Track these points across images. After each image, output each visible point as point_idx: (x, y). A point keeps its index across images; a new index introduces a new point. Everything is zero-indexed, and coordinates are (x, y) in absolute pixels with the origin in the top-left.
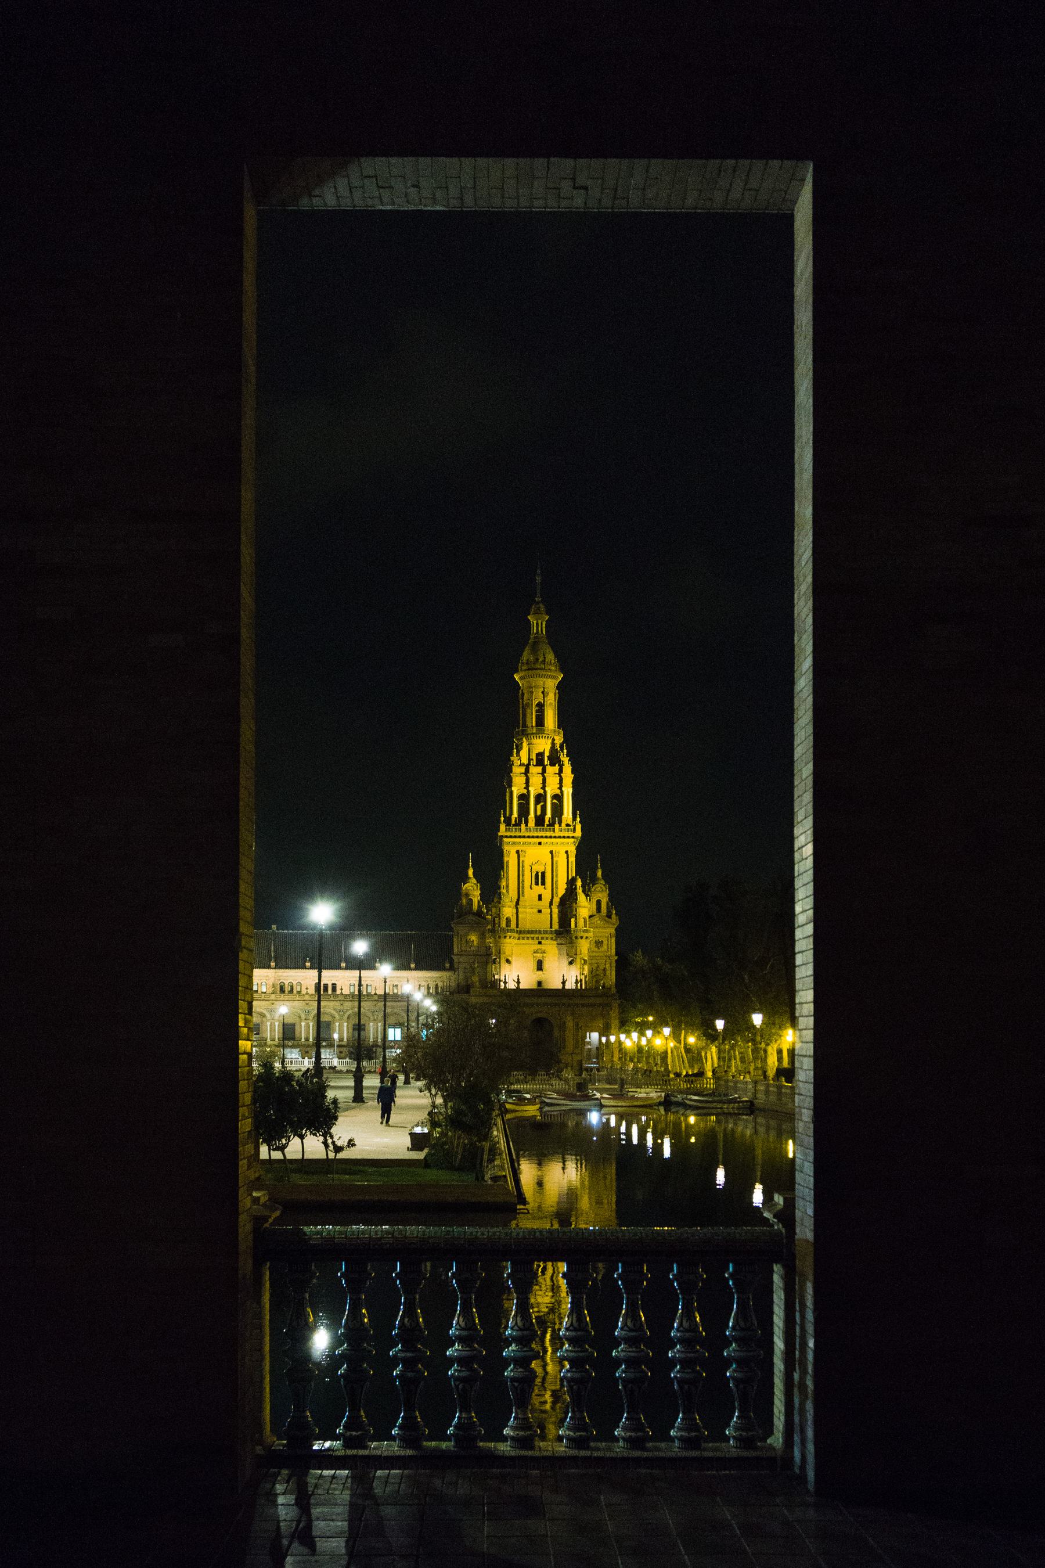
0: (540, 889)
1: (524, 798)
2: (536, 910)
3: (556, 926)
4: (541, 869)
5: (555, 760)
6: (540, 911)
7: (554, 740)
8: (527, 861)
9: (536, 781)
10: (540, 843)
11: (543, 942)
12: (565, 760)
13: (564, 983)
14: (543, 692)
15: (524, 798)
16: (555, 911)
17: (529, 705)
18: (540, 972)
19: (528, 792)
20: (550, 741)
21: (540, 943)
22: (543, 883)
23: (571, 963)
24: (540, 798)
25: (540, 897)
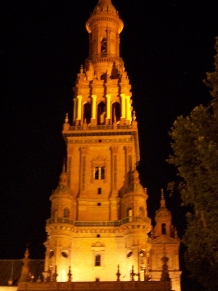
0: (100, 183)
1: (88, 108)
2: (96, 203)
3: (115, 218)
4: (100, 163)
5: (116, 75)
6: (99, 204)
7: (114, 63)
8: (89, 158)
9: (98, 90)
10: (100, 141)
11: (102, 235)
12: (124, 75)
13: (118, 274)
14: (106, 31)
15: (88, 108)
16: (114, 202)
17: (96, 41)
18: (98, 268)
19: (92, 99)
20: (111, 65)
21: (98, 236)
22: (103, 177)
23: (129, 255)
24: (102, 107)
25: (100, 191)
